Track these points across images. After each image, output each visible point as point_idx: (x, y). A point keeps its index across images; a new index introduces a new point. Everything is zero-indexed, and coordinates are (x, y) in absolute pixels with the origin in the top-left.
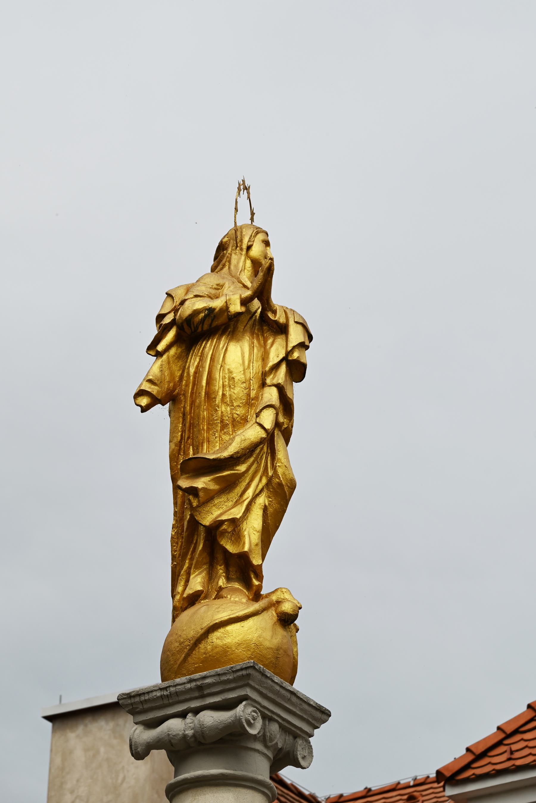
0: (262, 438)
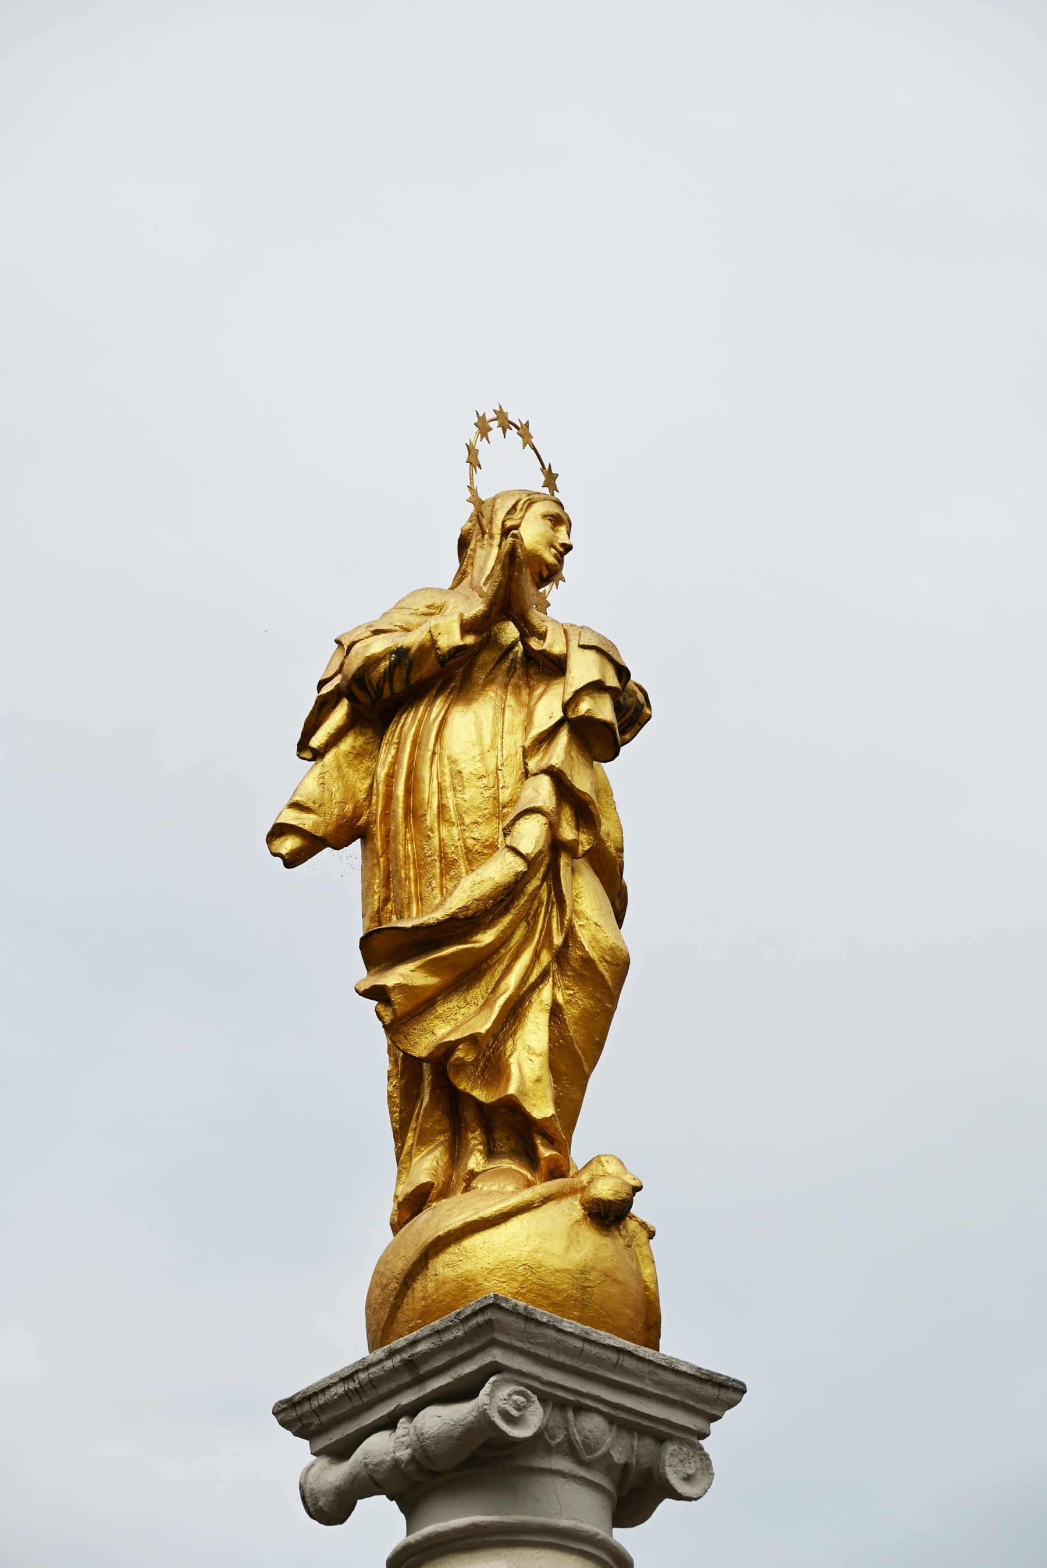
0: (517, 874)
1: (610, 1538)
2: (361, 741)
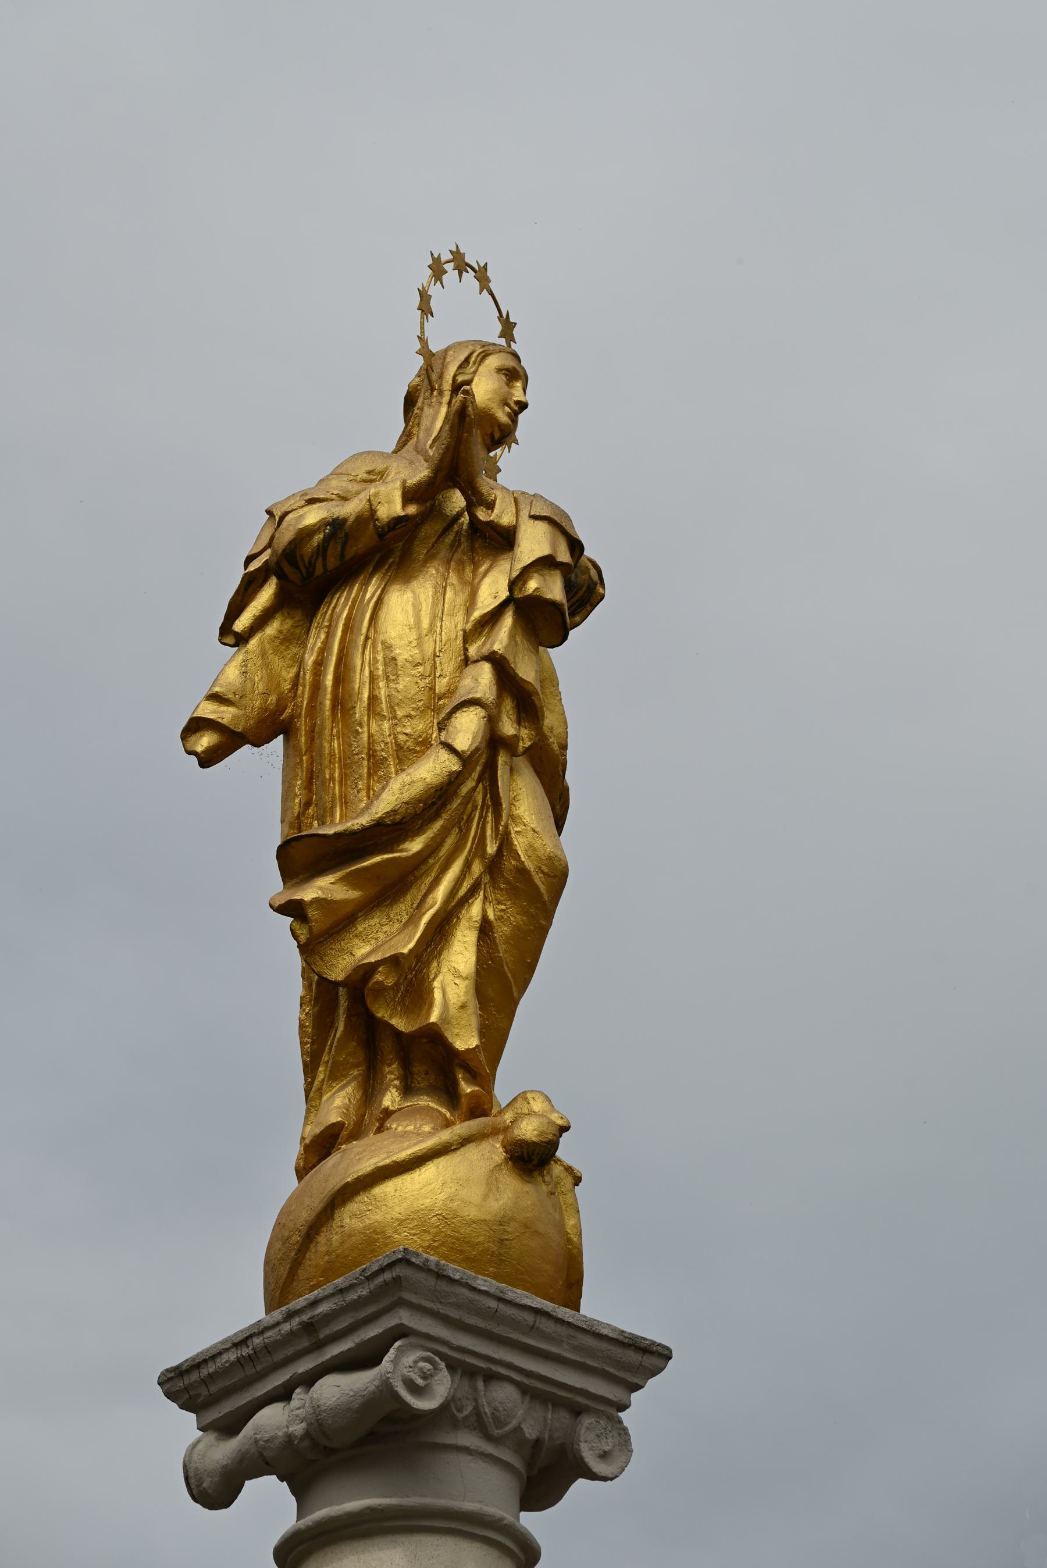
1: (517, 1524)
2: (289, 624)
